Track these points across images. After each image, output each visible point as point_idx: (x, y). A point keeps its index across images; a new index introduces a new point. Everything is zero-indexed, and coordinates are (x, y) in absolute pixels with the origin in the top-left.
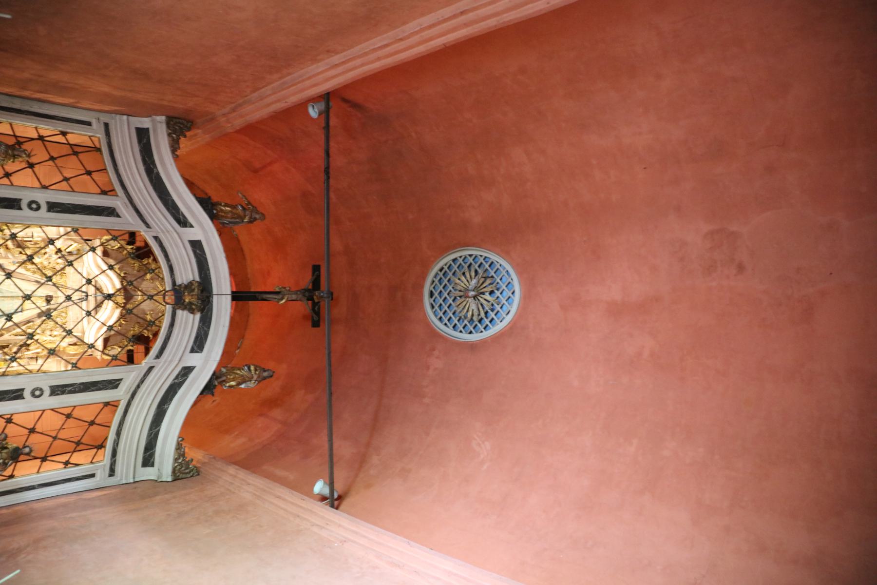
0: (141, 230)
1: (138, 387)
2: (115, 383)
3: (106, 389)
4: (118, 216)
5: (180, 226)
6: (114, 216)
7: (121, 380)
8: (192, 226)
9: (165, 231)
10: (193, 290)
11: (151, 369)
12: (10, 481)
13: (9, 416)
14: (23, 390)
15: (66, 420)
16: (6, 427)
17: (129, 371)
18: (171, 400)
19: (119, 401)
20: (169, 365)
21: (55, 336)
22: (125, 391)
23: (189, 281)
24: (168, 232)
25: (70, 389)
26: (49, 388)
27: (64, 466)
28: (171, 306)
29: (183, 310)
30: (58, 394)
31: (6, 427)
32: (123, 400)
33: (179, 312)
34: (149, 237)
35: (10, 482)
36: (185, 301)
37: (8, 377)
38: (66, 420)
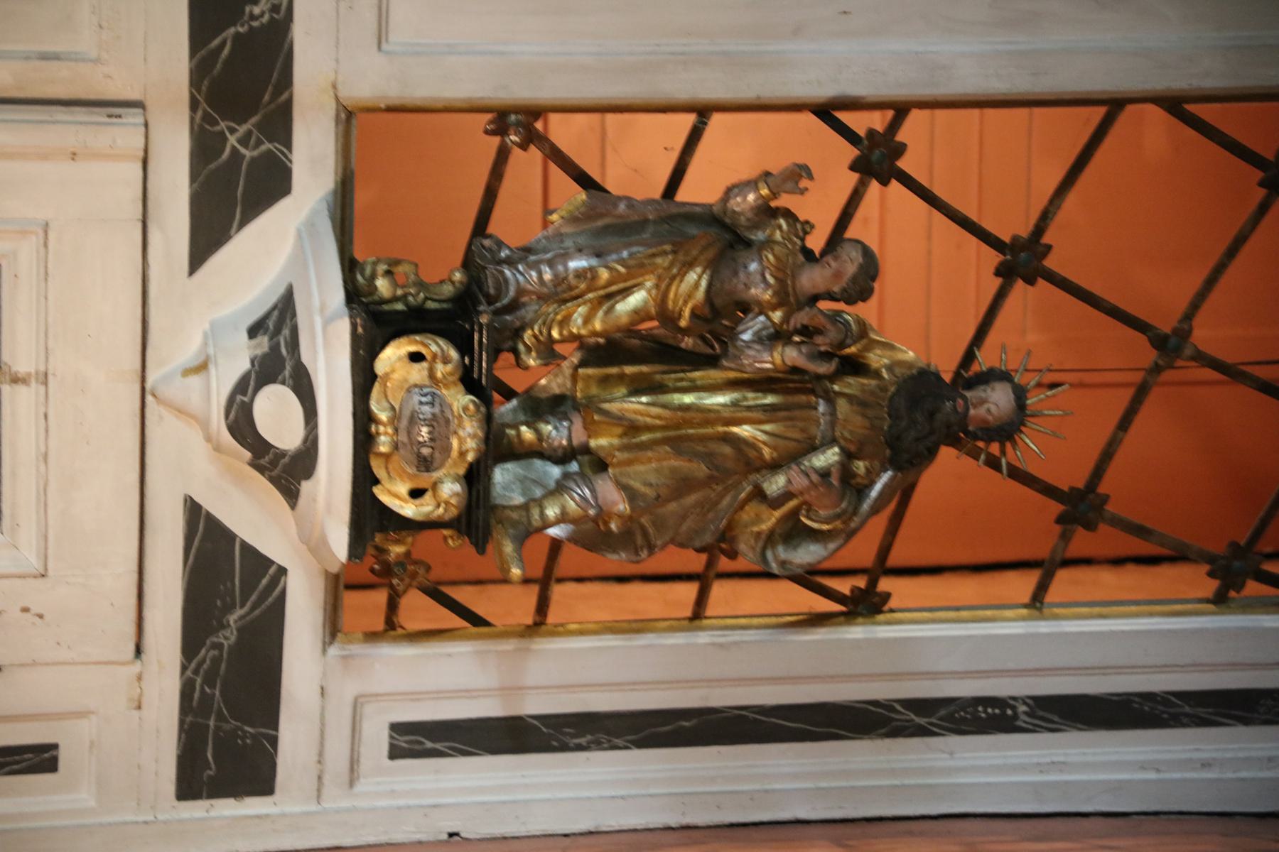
12: (857, 632)
13: (877, 121)
16: (855, 198)
27: (1211, 586)
31: (855, 198)
35: (856, 643)
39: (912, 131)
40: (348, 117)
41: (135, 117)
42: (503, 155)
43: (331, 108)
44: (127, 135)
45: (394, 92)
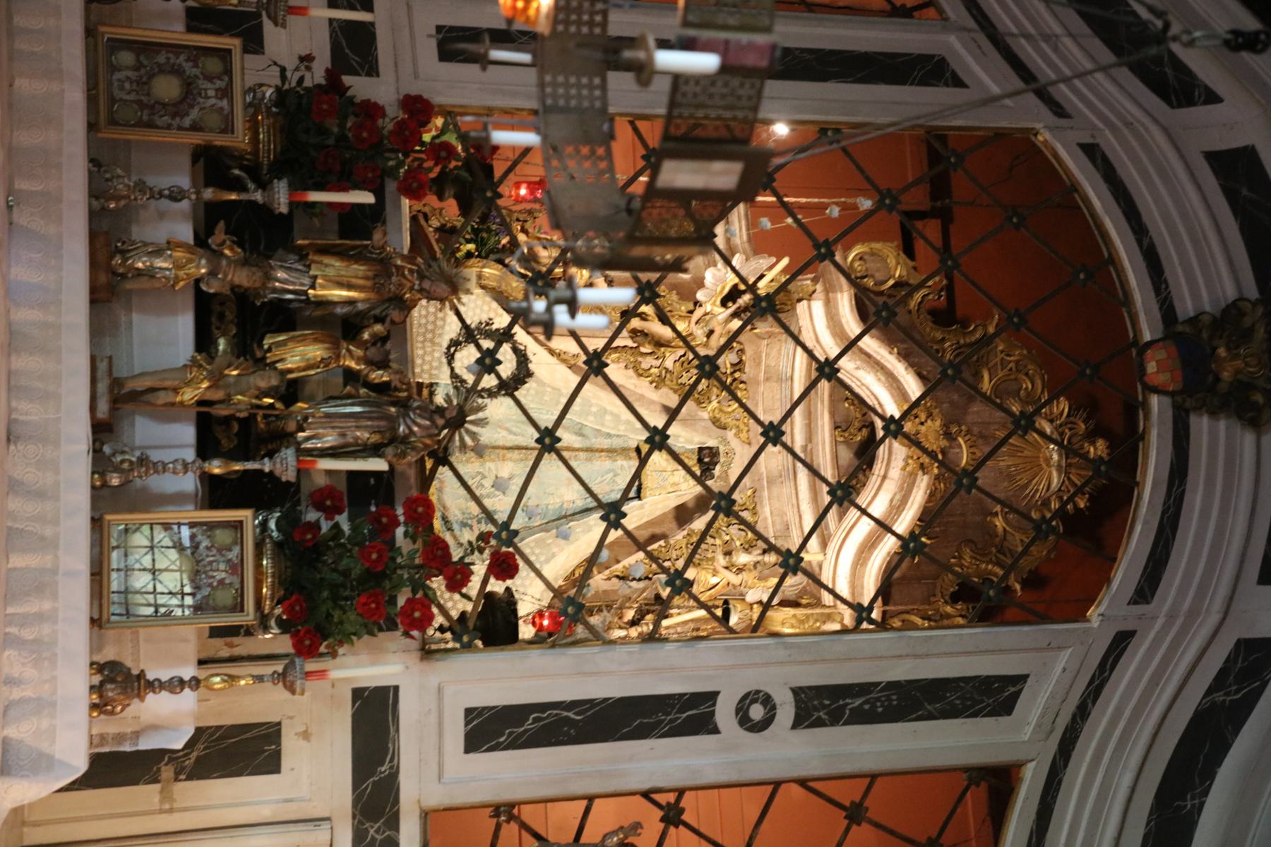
0: (1038, 126)
1: (1082, 712)
2: (1001, 690)
3: (974, 715)
4: (958, 82)
5: (1172, 107)
6: (947, 85)
7: (1023, 678)
8: (1212, 98)
9: (1119, 124)
10: (1247, 334)
11: (1122, 641)
13: (671, 797)
14: (712, 697)
15: (848, 829)
17: (1049, 647)
18: (1209, 776)
19: (1019, 766)
20: (1184, 630)
21: (740, 570)
22: (1039, 725)
23: (1223, 305)
24: (1128, 125)
25: (858, 702)
26: (790, 696)
28: (1167, 400)
29: (1213, 414)
30: (819, 723)
32: (1031, 766)
33: (1201, 425)
34: (1064, 146)
36: (1218, 379)
37: (669, 647)
38: (848, 829)
39: (688, 801)
40: (426, 815)
41: (326, 825)
42: (498, 827)
43: (418, 813)
44: (322, 835)
45: (447, 802)
